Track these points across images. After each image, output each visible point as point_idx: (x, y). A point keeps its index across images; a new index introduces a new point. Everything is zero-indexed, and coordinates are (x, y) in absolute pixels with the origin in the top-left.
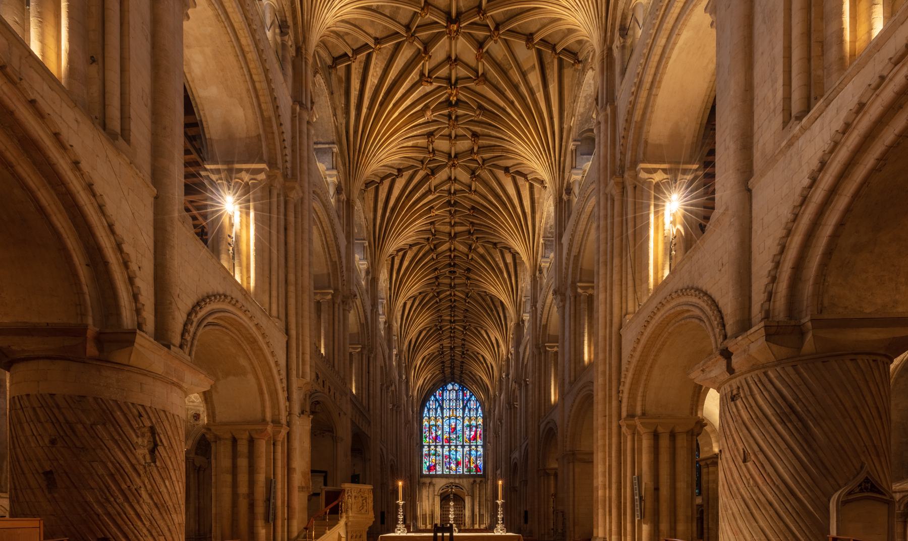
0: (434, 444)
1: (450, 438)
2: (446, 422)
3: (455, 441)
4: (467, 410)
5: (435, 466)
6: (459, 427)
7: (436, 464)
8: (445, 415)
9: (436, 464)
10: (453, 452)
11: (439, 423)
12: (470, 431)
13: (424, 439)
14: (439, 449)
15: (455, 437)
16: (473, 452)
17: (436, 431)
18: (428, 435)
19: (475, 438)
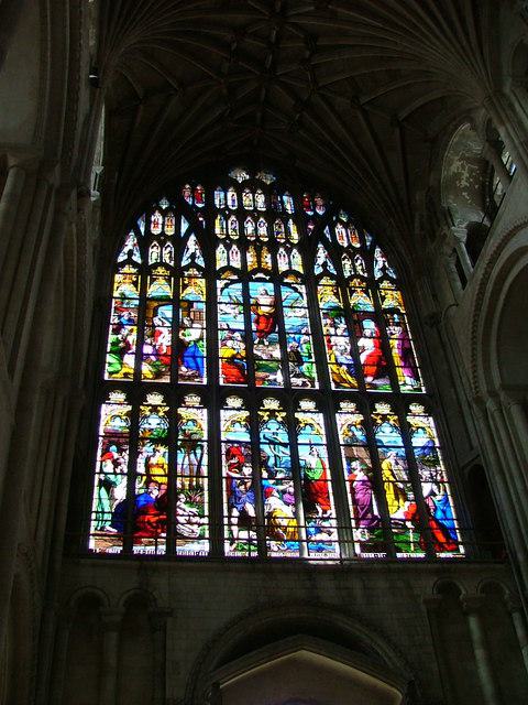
0: (166, 380)
1: (251, 357)
2: (230, 292)
3: (279, 377)
4: (322, 255)
5: (167, 503)
6: (295, 318)
7: (171, 494)
8: (220, 264)
9: (171, 494)
10: (273, 429)
11: (195, 291)
12: (355, 332)
13: (110, 358)
14: (194, 416)
15: (277, 354)
16: (388, 435)
17: (177, 326)
18: (132, 339)
19: (384, 367)
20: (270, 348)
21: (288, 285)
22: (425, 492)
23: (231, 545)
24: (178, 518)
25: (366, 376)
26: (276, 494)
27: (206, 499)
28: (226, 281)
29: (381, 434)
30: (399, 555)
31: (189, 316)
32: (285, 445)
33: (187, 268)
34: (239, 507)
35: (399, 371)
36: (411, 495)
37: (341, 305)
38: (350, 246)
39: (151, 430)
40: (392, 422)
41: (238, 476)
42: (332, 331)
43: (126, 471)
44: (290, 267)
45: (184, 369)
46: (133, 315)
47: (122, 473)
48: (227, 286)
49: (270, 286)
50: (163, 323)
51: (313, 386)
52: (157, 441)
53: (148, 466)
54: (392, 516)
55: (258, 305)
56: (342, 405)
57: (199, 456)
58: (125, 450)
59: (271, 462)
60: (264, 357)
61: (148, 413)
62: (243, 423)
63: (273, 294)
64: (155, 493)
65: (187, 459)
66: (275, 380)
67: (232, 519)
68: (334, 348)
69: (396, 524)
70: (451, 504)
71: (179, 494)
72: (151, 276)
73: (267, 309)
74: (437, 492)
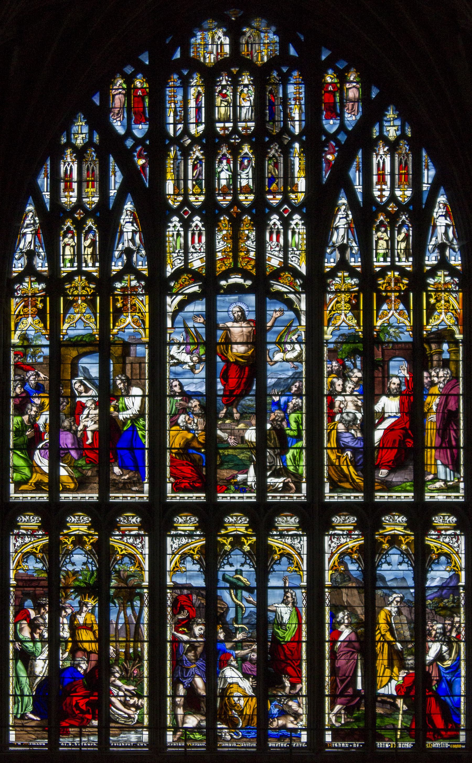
18: (43, 420)
20: (241, 426)
21: (279, 296)
22: (431, 655)
23: (174, 734)
24: (113, 699)
25: (379, 467)
26: (234, 663)
27: (146, 673)
28: (179, 298)
29: (385, 566)
30: (380, 744)
31: (123, 372)
32: (249, 589)
33: (120, 276)
34: (186, 681)
35: (430, 455)
36: (410, 661)
37: (360, 331)
38: (393, 198)
39: (75, 573)
40: (404, 547)
41: (185, 638)
42: (339, 382)
43: (46, 635)
44: (286, 258)
45: (117, 470)
46: (42, 375)
47: (42, 640)
48: (182, 305)
49: (252, 299)
50: (87, 390)
51: (299, 490)
52: (80, 591)
53: (74, 628)
54: (381, 691)
55: (228, 342)
56: (336, 520)
57: (137, 609)
58: (43, 606)
59: (231, 614)
60: (231, 441)
61: (70, 547)
62: (196, 557)
63: (252, 316)
64: (83, 667)
65: (122, 615)
66: (245, 482)
67: (178, 699)
68: (338, 417)
69: (383, 702)
70: (463, 673)
71: (111, 666)
72: (66, 295)
73: (239, 349)
74: (447, 657)
